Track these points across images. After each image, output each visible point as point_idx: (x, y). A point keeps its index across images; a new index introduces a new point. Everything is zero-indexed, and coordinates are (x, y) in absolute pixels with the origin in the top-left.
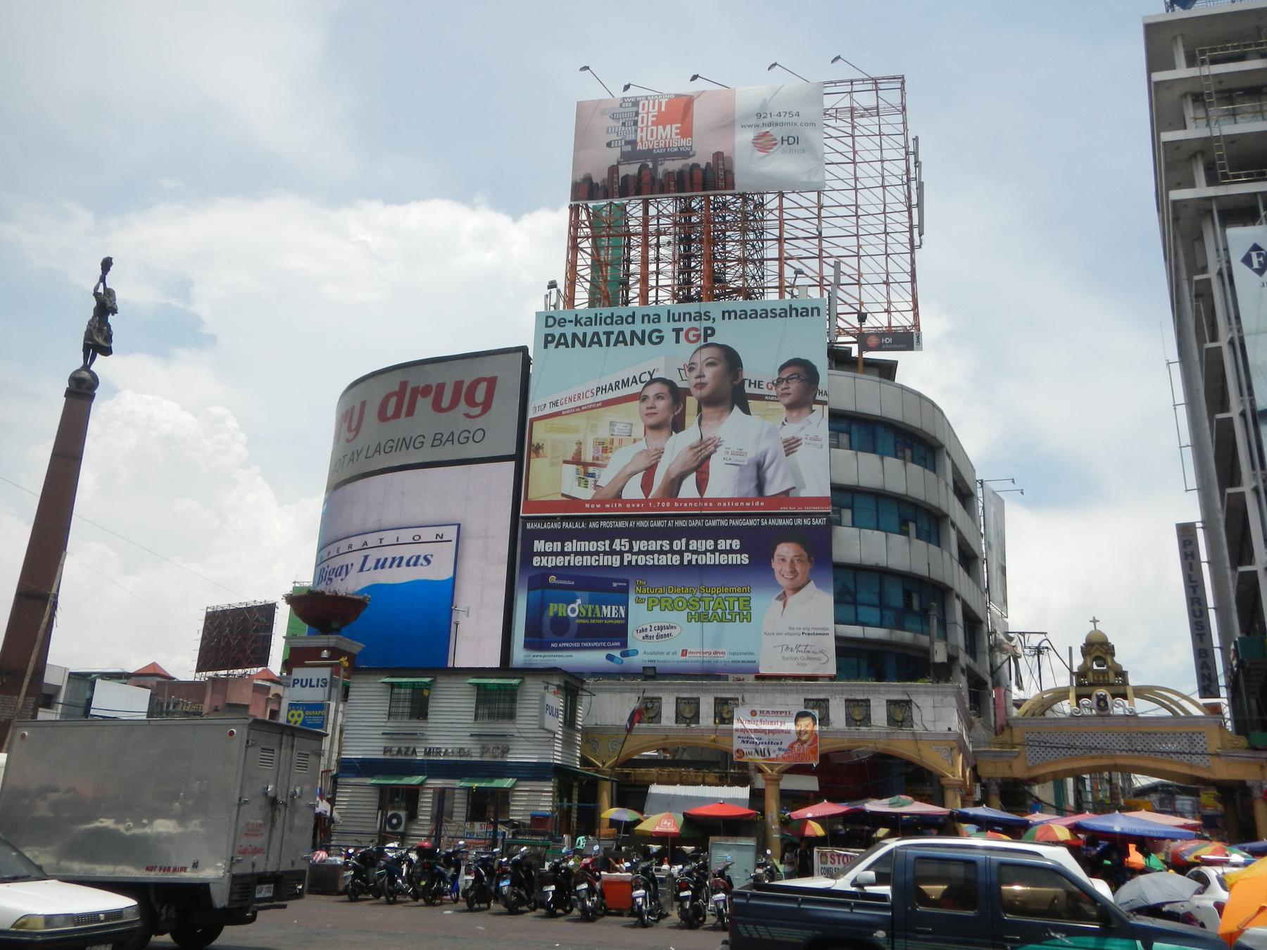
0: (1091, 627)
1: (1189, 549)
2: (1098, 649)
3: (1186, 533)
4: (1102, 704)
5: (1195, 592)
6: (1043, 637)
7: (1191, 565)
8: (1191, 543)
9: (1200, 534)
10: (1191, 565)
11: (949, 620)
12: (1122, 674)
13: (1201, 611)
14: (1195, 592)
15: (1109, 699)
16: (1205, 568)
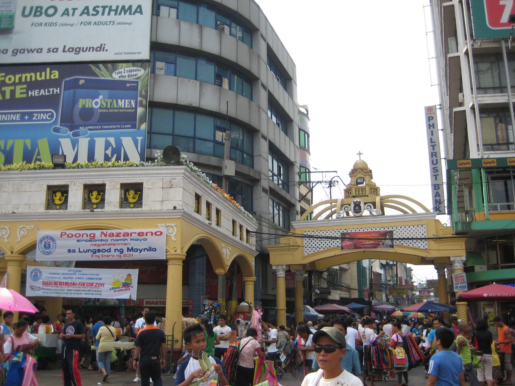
0: (357, 158)
1: (431, 122)
2: (361, 172)
3: (430, 112)
4: (357, 208)
5: (434, 149)
6: (334, 174)
7: (432, 132)
8: (433, 118)
9: (439, 112)
10: (432, 132)
11: (256, 153)
12: (375, 190)
13: (437, 160)
14: (434, 149)
15: (362, 205)
16: (441, 134)
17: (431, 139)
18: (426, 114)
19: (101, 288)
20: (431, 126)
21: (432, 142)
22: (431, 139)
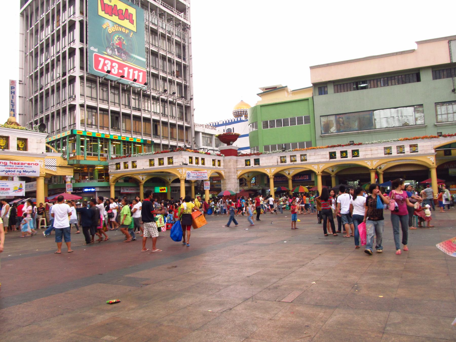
1: (13, 90)
5: (13, 107)
7: (13, 96)
8: (14, 88)
10: (13, 96)
14: (13, 107)
17: (12, 101)
18: (10, 84)
19: (9, 191)
20: (13, 93)
21: (12, 102)
22: (12, 101)
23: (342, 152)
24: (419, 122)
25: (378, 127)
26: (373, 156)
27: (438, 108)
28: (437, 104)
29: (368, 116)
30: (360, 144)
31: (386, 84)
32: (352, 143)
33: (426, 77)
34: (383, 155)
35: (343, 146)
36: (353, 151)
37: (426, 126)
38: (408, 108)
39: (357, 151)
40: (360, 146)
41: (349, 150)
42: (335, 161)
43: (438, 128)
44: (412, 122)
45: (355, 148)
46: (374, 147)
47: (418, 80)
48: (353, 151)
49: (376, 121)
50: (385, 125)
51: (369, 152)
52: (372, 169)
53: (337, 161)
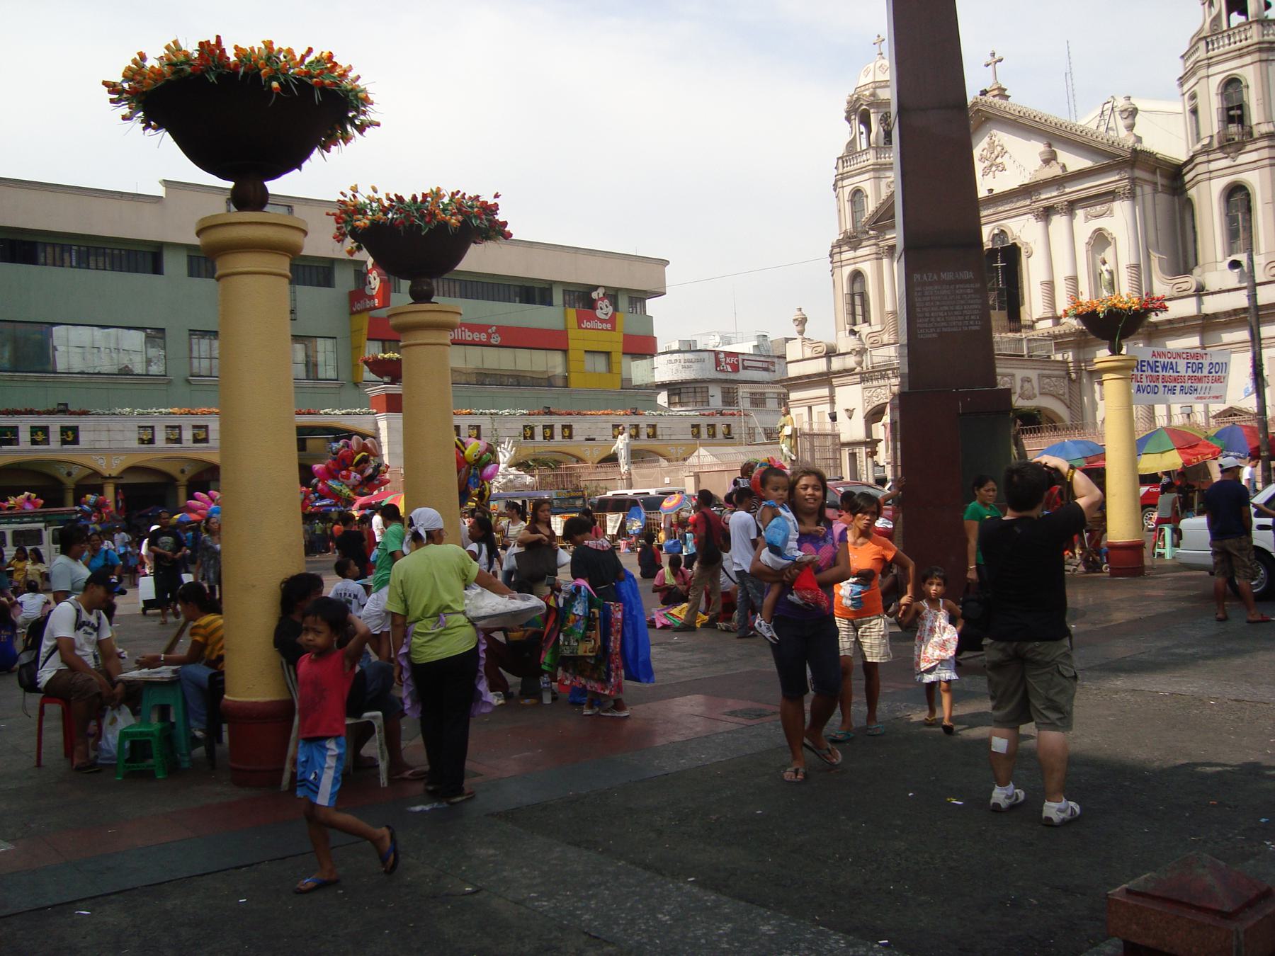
23: (34, 430)
24: (155, 369)
25: (61, 366)
26: (113, 445)
27: (195, 341)
28: (193, 332)
29: (38, 337)
30: (85, 413)
31: (83, 263)
32: (64, 410)
33: (175, 265)
34: (136, 444)
35: (39, 413)
36: (64, 430)
37: (170, 382)
38: (132, 332)
39: (75, 430)
40: (83, 418)
41: (56, 424)
42: (17, 451)
43: (193, 388)
44: (139, 368)
45: (69, 421)
46: (115, 423)
47: (157, 269)
48: (64, 430)
49: (57, 353)
50: (77, 366)
51: (104, 436)
52: (110, 477)
53: (21, 451)
